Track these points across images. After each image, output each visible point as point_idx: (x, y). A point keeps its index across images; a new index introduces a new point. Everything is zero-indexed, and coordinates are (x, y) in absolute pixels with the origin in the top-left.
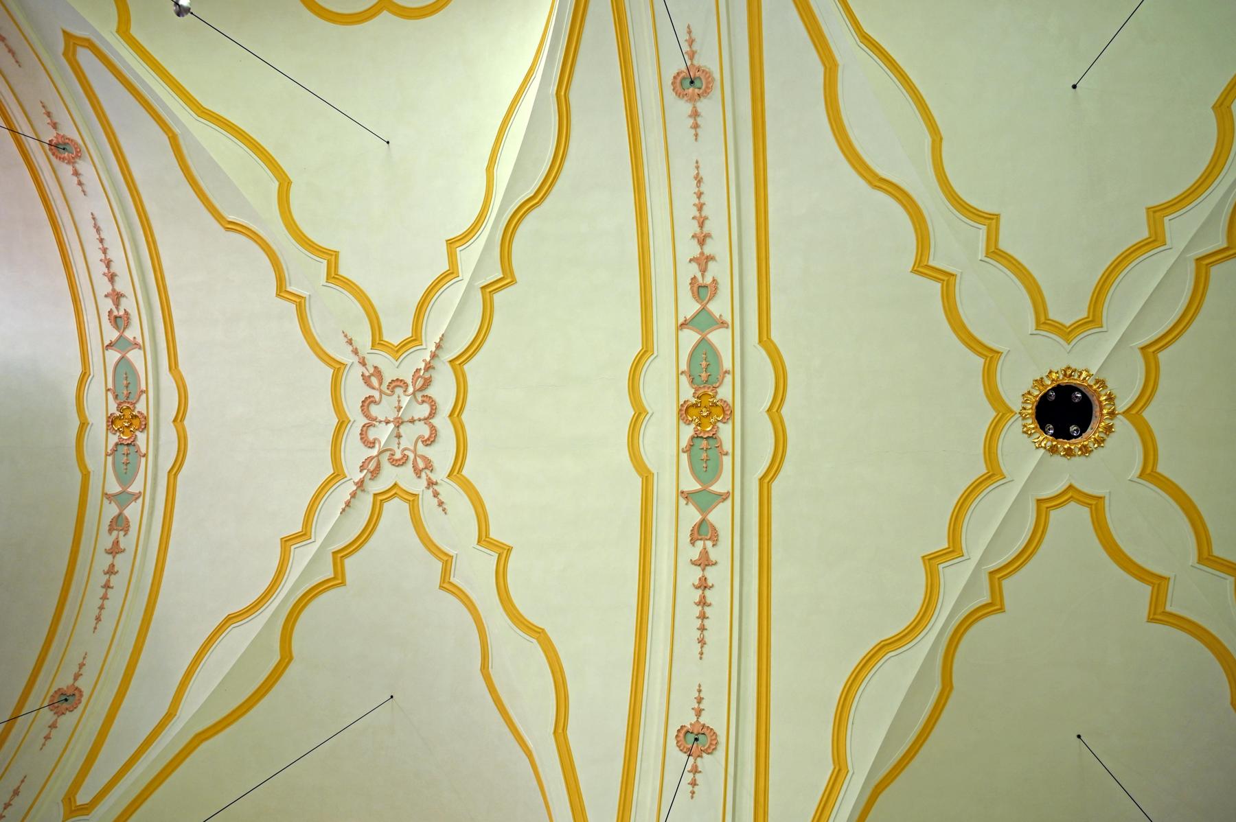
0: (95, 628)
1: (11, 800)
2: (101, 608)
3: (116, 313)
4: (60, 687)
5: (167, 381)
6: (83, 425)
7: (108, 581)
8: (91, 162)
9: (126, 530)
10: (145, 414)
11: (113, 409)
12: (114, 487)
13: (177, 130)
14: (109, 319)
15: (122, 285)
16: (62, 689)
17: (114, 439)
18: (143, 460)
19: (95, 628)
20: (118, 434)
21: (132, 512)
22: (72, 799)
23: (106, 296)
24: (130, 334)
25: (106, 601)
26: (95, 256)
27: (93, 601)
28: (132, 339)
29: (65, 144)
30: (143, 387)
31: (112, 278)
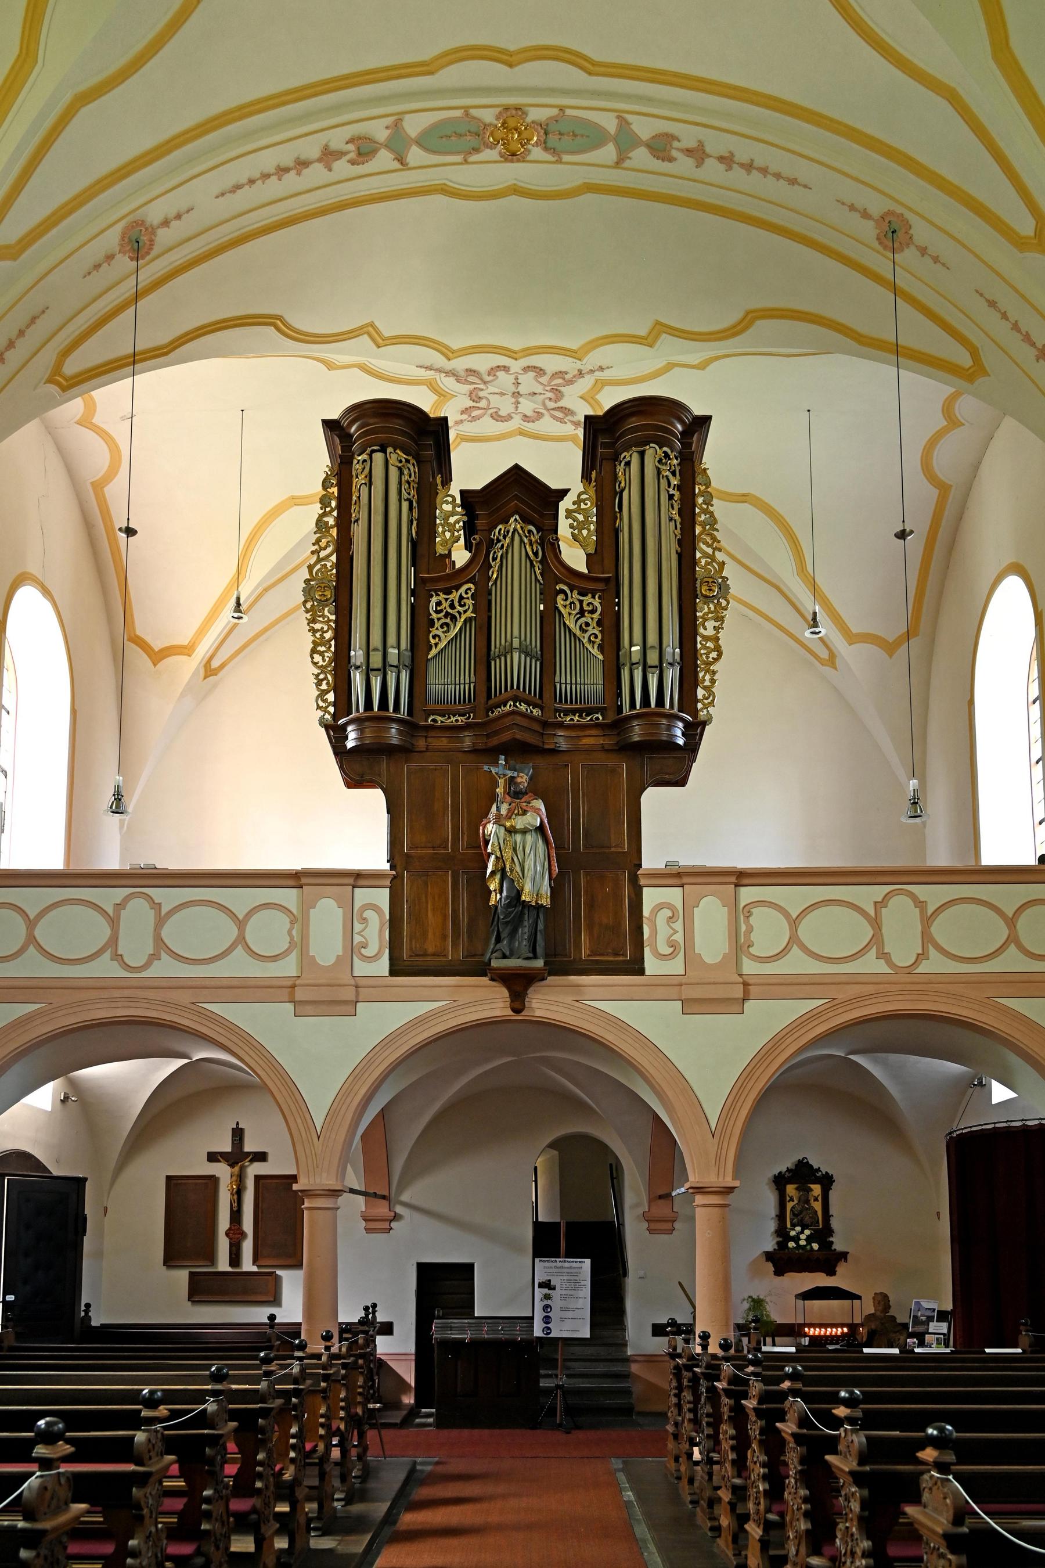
0: (805, 186)
1: (1000, 311)
2: (778, 176)
3: (352, 155)
4: (876, 236)
5: (451, 76)
6: (516, 191)
7: (742, 165)
8: (146, 207)
9: (672, 137)
10: (500, 109)
11: (492, 154)
12: (608, 153)
13: (68, 97)
14: (363, 164)
15: (311, 149)
16: (878, 235)
17: (537, 153)
18: (568, 112)
19: (805, 186)
20: (530, 147)
21: (644, 129)
22: (1023, 241)
23: (330, 170)
24: (382, 134)
25: (770, 170)
26: (274, 188)
27: (769, 187)
28: (388, 132)
29: (130, 241)
30: (458, 113)
31: (302, 164)
